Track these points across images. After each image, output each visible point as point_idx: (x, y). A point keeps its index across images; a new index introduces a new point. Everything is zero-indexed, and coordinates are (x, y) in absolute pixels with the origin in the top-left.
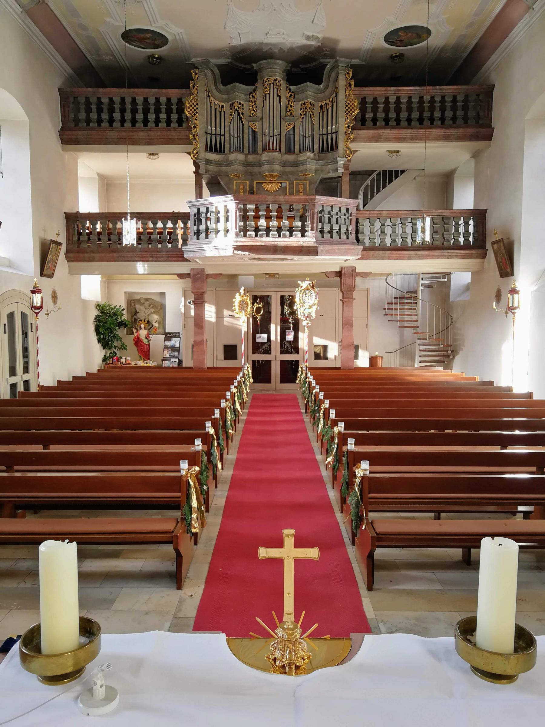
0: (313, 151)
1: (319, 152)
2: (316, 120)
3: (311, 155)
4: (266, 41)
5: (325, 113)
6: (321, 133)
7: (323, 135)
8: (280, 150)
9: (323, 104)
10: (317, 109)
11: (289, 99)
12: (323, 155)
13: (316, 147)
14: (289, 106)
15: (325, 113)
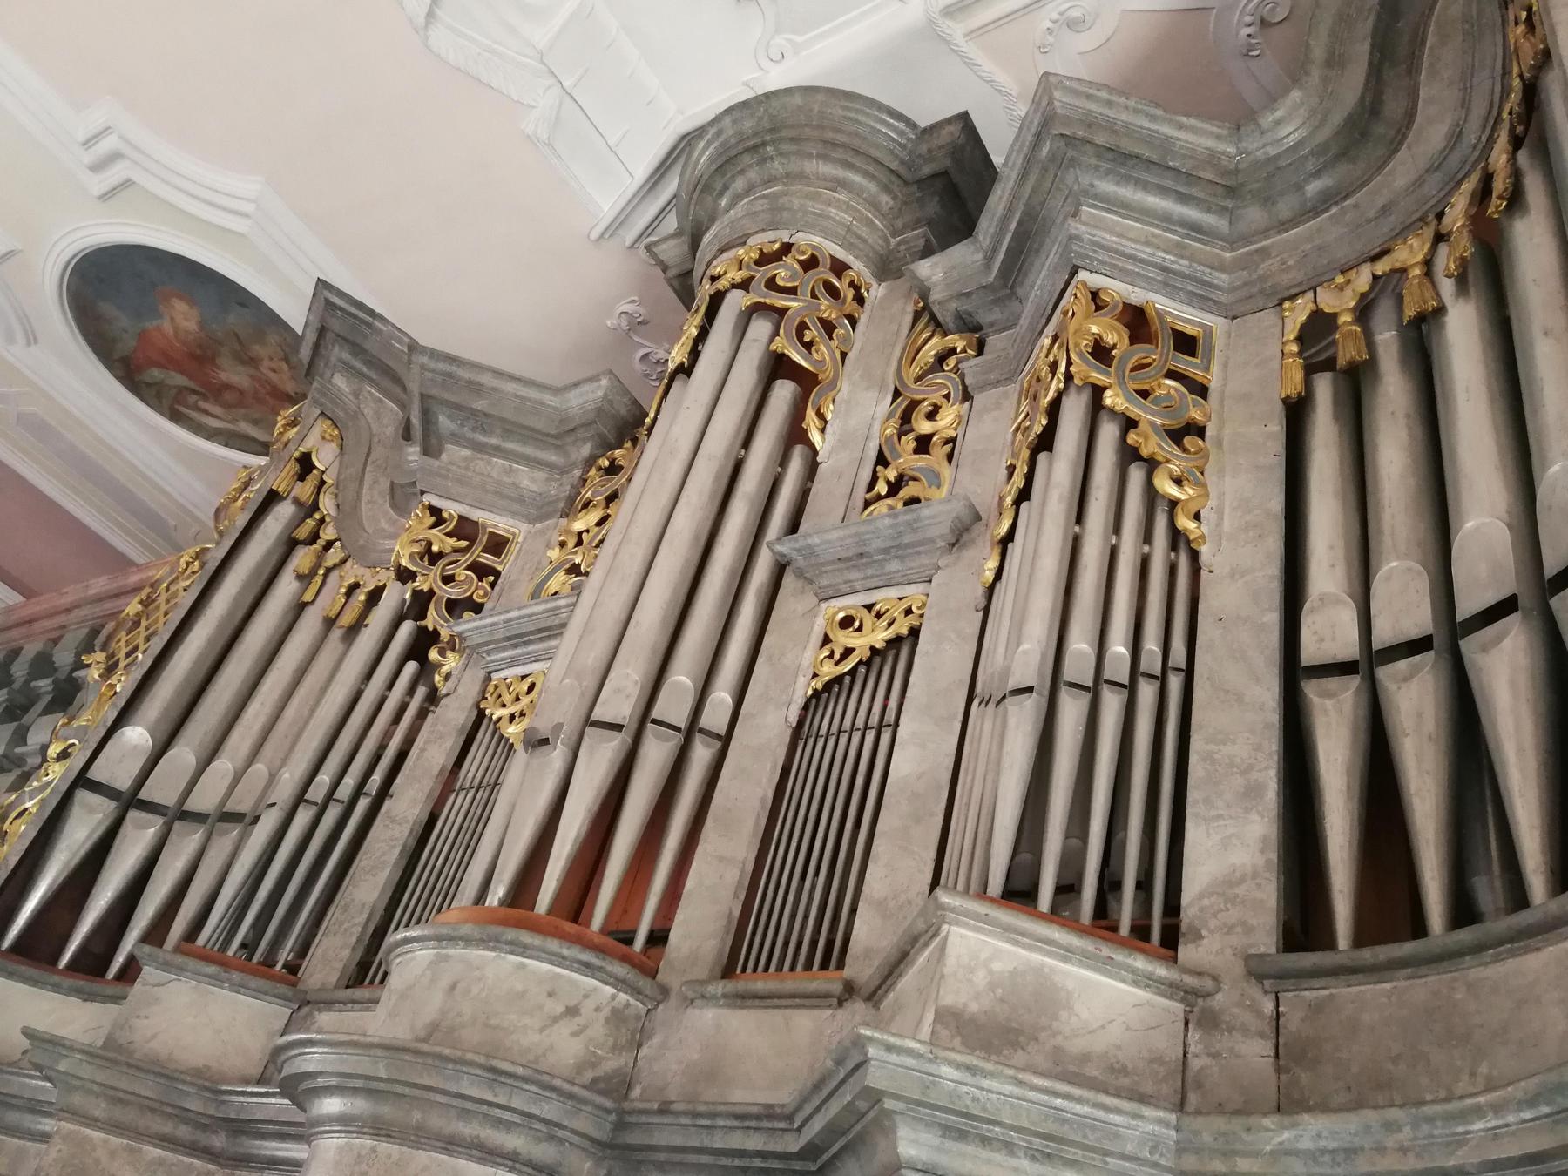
0: (1163, 931)
1: (1304, 920)
2: (1231, 507)
3: (1106, 997)
4: (776, 79)
5: (1393, 393)
6: (1330, 631)
7: (1367, 664)
8: (658, 938)
9: (1339, 302)
10: (1250, 367)
11: (914, 391)
12: (1370, 1005)
13: (1229, 850)
14: (909, 442)
15: (1393, 393)
